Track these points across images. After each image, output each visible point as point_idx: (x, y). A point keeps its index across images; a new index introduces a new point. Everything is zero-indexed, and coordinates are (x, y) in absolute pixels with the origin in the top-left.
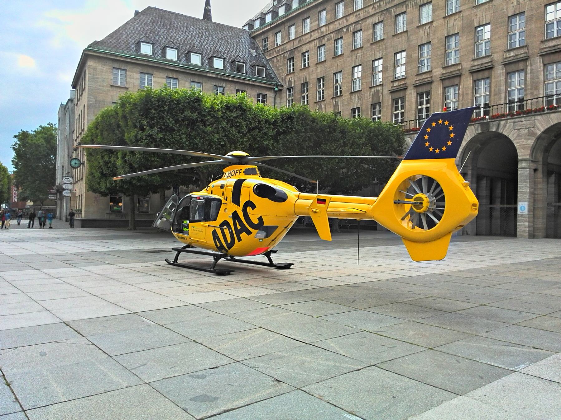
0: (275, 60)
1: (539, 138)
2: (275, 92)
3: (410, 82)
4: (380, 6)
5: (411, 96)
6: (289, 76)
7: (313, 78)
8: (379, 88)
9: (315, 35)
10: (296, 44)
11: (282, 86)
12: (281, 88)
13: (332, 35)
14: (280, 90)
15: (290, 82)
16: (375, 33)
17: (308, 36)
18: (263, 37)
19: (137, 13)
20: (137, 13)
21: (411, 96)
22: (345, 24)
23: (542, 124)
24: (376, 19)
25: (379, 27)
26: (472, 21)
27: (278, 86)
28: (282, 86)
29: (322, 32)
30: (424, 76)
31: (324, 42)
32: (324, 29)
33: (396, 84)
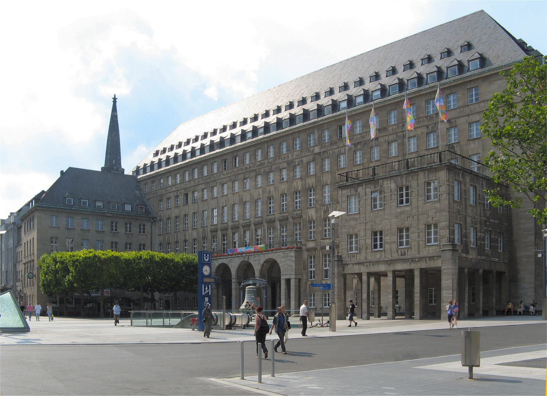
0: (152, 199)
1: (263, 266)
2: (152, 223)
3: (219, 227)
4: (205, 179)
5: (219, 234)
6: (160, 212)
7: (173, 215)
8: (206, 228)
9: (174, 189)
10: (163, 192)
11: (156, 218)
12: (155, 219)
13: (183, 191)
14: (155, 221)
15: (160, 216)
16: (203, 195)
17: (170, 188)
18: (144, 182)
19: (62, 172)
20: (62, 172)
21: (219, 234)
22: (189, 186)
23: (263, 258)
24: (203, 186)
25: (205, 191)
26: (242, 199)
27: (153, 218)
28: (156, 218)
29: (178, 187)
30: (224, 225)
31: (178, 194)
32: (178, 186)
33: (213, 227)
